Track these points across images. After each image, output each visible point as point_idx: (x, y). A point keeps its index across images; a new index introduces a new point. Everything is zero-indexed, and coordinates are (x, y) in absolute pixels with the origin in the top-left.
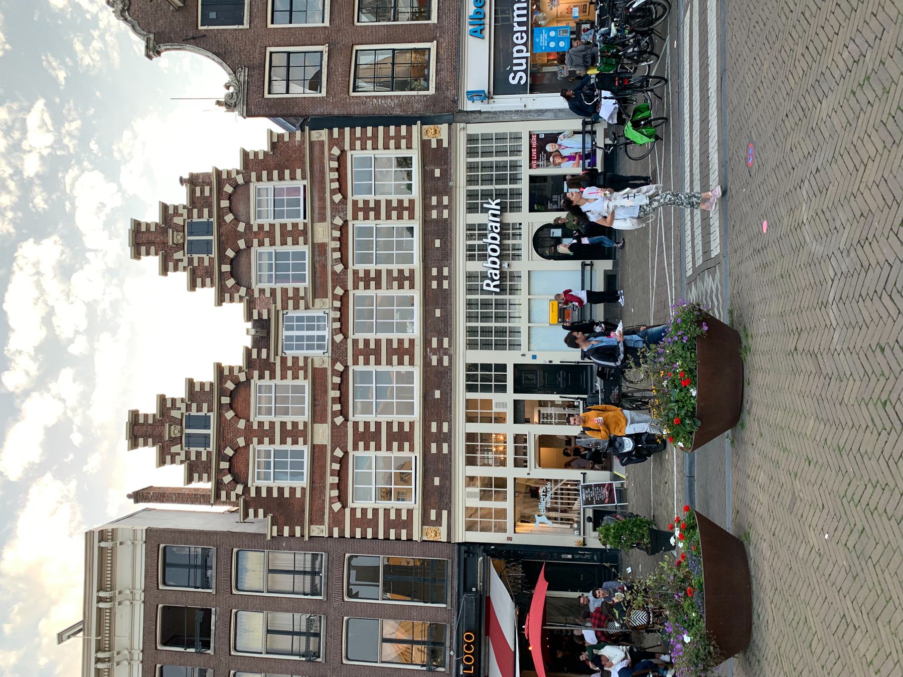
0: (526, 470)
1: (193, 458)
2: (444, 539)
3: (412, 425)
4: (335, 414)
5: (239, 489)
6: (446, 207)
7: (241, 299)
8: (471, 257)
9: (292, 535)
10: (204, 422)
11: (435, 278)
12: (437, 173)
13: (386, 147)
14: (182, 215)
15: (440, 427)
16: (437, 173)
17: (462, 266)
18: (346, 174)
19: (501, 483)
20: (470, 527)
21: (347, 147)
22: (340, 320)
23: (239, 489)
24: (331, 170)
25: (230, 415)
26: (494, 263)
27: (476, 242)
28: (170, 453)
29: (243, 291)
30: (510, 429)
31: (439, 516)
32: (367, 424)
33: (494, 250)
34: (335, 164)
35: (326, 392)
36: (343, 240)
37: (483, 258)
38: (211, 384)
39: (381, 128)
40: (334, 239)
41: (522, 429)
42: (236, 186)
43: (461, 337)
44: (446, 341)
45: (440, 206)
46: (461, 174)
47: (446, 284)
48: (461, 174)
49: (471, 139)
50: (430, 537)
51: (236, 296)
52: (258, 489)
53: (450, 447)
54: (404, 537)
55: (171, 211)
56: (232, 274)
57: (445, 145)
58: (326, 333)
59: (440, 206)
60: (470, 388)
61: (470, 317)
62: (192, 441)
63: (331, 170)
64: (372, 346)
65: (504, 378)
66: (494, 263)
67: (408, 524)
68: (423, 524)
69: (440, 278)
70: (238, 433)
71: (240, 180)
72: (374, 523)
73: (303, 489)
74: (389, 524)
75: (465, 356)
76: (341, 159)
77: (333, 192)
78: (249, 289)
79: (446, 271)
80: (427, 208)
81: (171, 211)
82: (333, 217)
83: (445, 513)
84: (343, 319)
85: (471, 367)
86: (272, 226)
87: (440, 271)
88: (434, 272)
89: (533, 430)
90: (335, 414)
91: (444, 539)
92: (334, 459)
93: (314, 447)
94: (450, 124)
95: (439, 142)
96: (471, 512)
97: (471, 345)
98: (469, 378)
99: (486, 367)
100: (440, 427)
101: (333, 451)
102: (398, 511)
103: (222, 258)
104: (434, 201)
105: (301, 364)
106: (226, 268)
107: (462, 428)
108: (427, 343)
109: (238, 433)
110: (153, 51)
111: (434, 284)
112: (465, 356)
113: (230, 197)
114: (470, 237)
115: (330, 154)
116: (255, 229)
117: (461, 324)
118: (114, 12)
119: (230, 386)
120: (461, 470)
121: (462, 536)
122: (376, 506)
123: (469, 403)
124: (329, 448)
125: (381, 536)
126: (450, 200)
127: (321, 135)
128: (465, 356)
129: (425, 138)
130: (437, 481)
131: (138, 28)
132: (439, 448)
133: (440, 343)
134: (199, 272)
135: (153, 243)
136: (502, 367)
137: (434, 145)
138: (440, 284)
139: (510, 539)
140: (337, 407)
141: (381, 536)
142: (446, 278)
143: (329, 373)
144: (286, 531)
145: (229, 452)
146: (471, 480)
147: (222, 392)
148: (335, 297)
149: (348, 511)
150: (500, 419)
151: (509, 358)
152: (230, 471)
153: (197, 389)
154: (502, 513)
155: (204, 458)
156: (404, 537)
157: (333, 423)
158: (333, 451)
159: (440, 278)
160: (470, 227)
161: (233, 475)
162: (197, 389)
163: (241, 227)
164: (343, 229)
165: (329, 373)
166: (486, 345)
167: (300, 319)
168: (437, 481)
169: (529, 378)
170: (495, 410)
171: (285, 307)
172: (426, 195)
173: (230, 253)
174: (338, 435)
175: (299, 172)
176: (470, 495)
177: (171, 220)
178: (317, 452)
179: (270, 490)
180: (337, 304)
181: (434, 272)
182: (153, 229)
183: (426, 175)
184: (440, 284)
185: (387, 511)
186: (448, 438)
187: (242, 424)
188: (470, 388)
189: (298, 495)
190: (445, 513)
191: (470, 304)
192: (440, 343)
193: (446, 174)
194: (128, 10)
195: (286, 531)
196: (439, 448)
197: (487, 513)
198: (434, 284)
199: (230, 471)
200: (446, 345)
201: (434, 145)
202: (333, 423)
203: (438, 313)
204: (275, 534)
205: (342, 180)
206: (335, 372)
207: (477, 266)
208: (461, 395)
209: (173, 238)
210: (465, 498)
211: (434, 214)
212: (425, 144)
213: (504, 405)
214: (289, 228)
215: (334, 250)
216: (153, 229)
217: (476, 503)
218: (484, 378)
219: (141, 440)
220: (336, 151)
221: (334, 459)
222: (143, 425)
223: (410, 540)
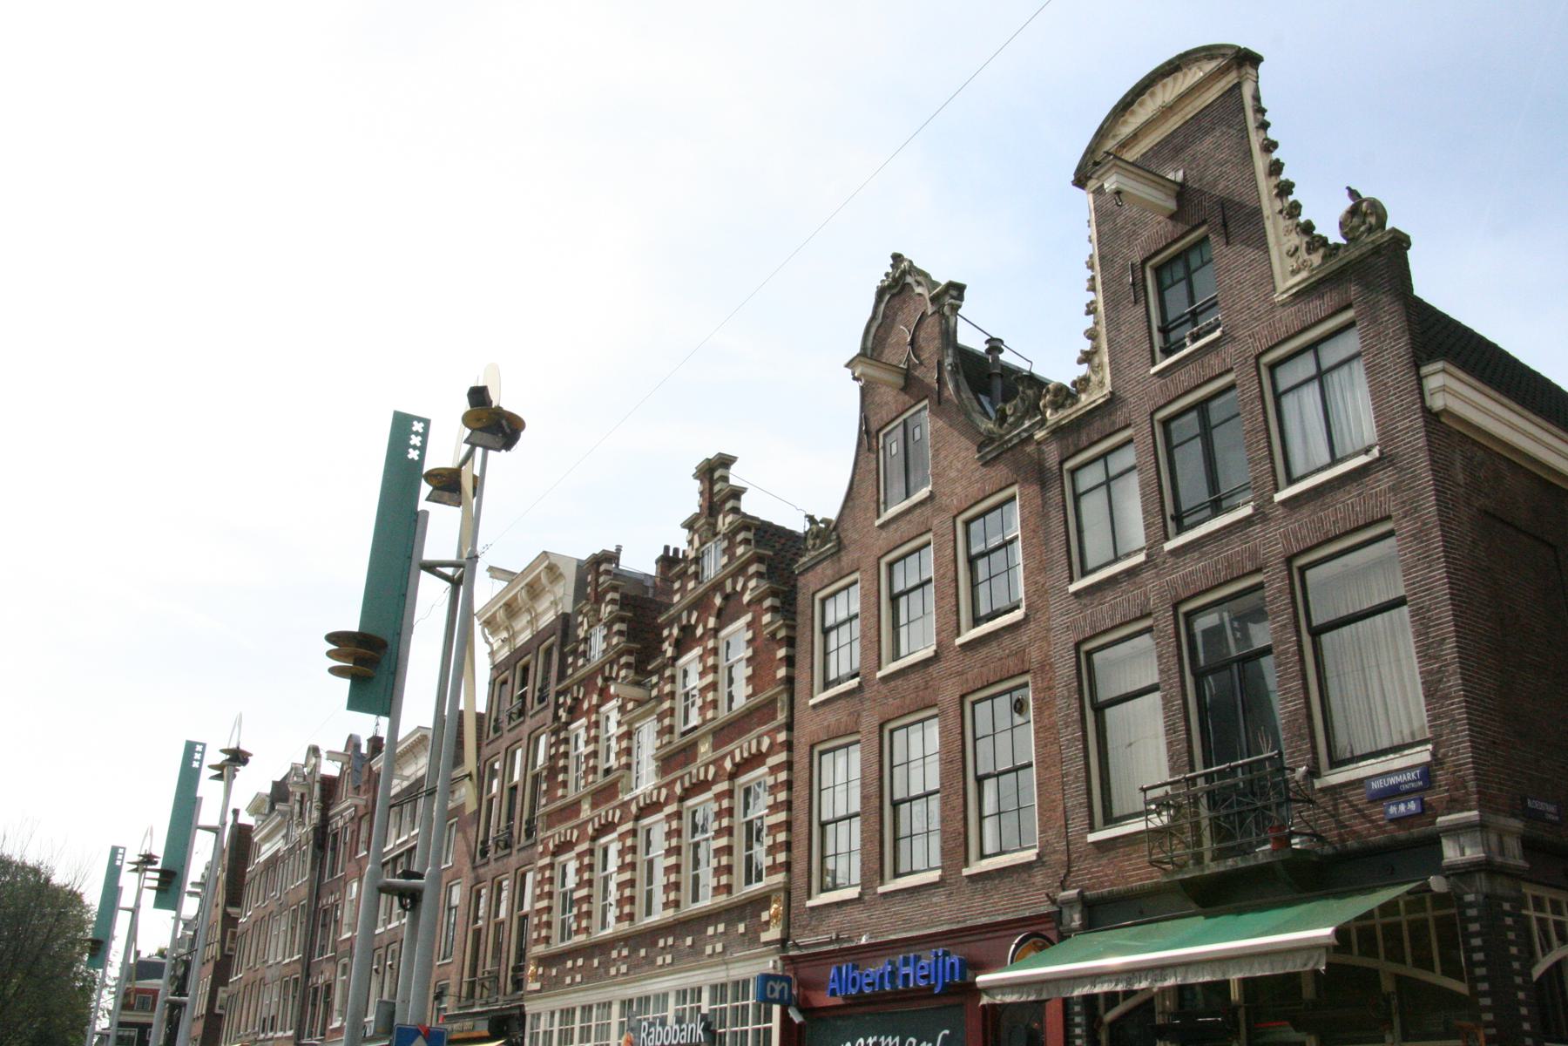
118: (887, 275)
131: (873, 330)
194: (893, 296)
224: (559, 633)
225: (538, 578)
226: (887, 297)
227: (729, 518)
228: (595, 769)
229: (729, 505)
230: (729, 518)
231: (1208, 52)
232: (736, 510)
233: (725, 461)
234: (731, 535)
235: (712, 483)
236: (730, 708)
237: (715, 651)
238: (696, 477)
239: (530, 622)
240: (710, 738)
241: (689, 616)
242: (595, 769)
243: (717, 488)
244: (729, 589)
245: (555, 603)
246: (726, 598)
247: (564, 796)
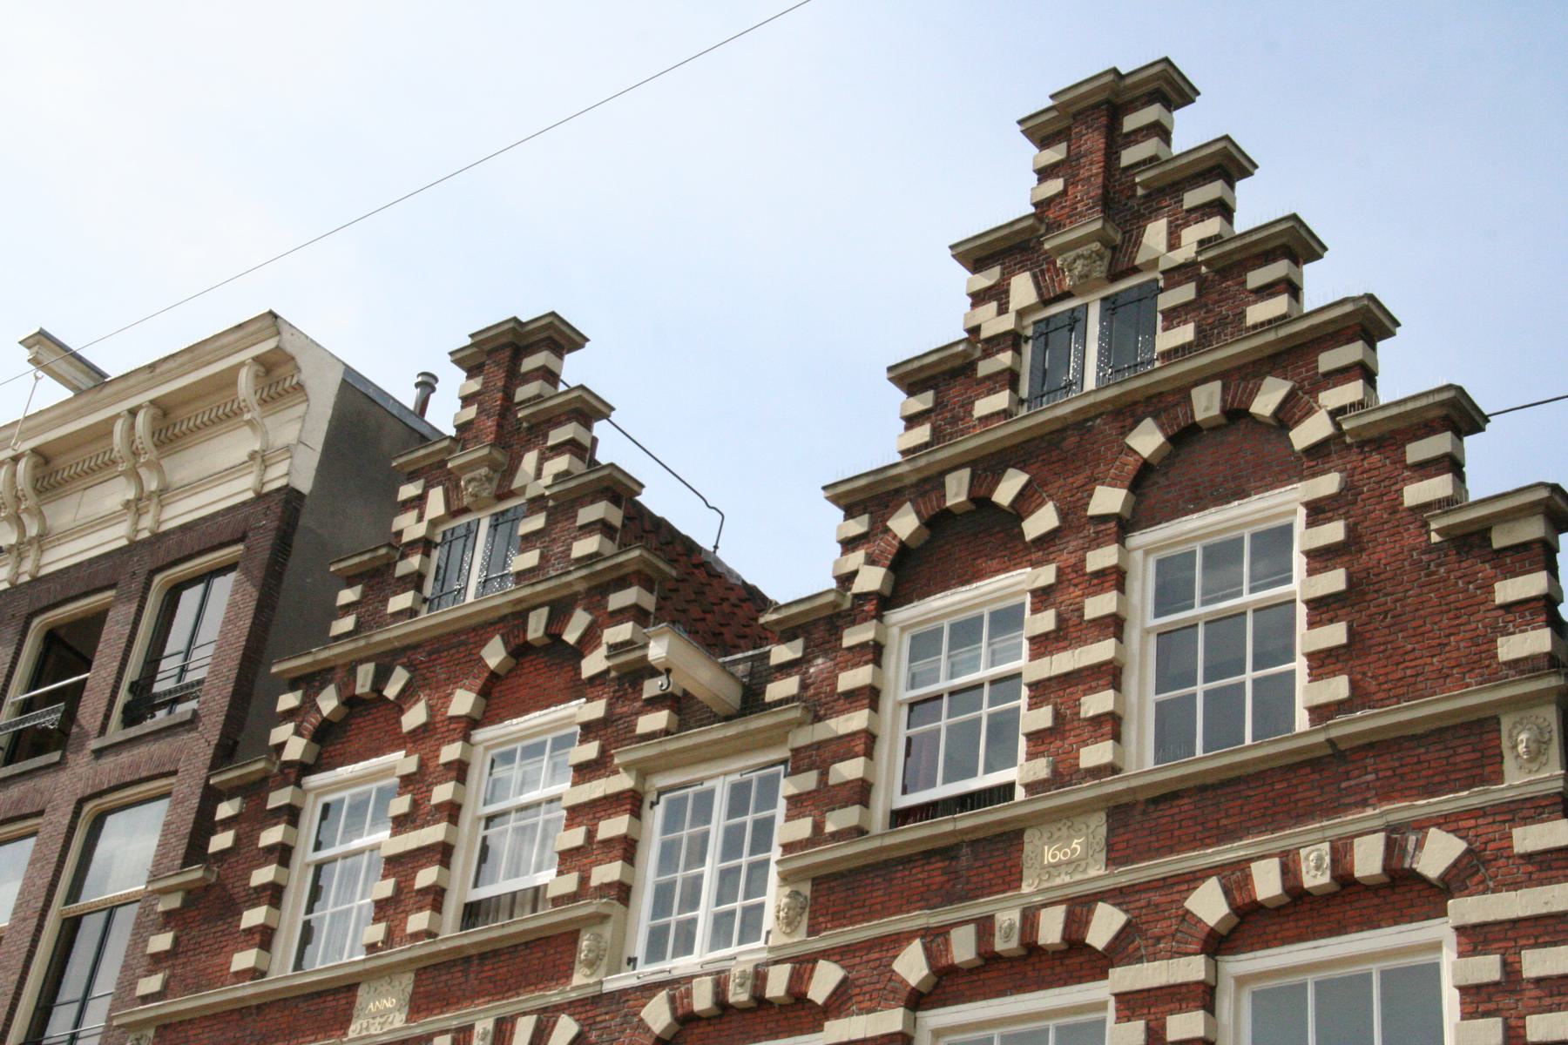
14: (1174, 243)
18: (1339, 929)
21: (1469, 908)
24: (1341, 852)
34: (1368, 860)
36: (1031, 966)
40: (1030, 918)
63: (1341, 852)
76: (1403, 893)
77: (1235, 878)
78: (884, 602)
113: (1235, 414)
115: (1421, 826)
143: (554, 996)
148: (803, 966)
164: (1076, 960)
165: (554, 996)
171: (799, 762)
180: (777, 984)
205: (1301, 913)
215: (985, 926)
220: (1437, 854)
224: (264, 544)
225: (227, 380)
227: (561, 463)
228: (435, 897)
229: (557, 436)
230: (561, 463)
232: (582, 450)
233: (558, 336)
234: (560, 506)
235: (514, 377)
236: (298, 965)
237: (459, 771)
238: (1040, 130)
239: (135, 507)
240: (407, 981)
241: (381, 677)
242: (435, 897)
243: (523, 392)
244: (363, 685)
245: (261, 458)
246: (351, 703)
247: (256, 973)
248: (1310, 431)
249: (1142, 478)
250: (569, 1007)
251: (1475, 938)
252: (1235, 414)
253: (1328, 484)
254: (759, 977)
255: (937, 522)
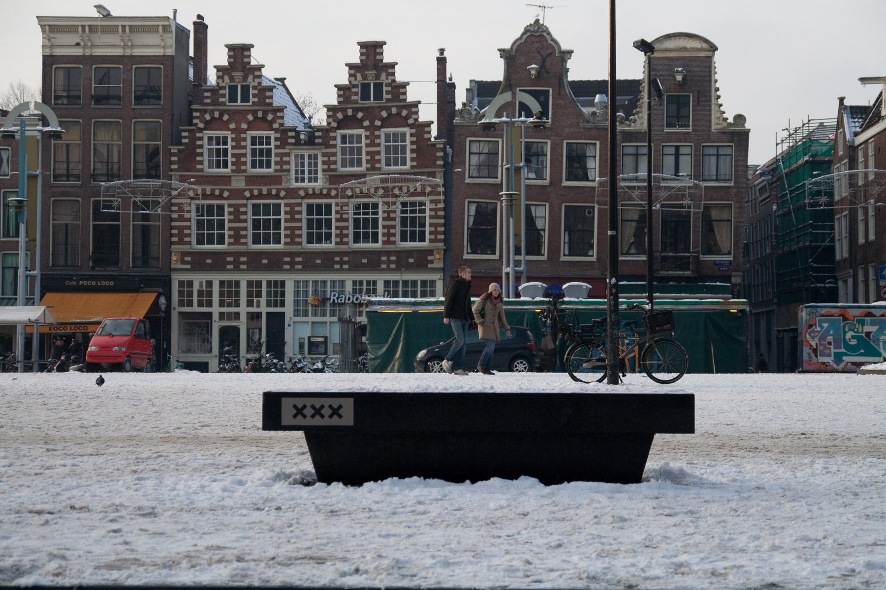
0: (217, 319)
1: (221, 92)
2: (173, 266)
3: (246, 244)
4: (251, 191)
5: (201, 125)
6: (388, 266)
7: (329, 124)
8: (355, 283)
9: (172, 163)
10: (245, 98)
11: (341, 259)
12: (411, 260)
13: (431, 225)
15: (243, 263)
16: (411, 260)
17: (349, 279)
19: (209, 304)
20: (181, 283)
22: (314, 193)
23: (201, 125)
25: (250, 117)
26: (349, 299)
27: (365, 287)
28: (224, 74)
29: (334, 125)
30: (243, 310)
31: (187, 263)
32: (245, 213)
33: (357, 299)
35: (265, 184)
37: (355, 291)
38: (271, 104)
39: (443, 221)
41: (243, 317)
42: (408, 117)
43: (302, 277)
44: (300, 267)
45: (389, 262)
46: (410, 277)
47: (337, 266)
48: (410, 277)
49: (433, 283)
50: (174, 258)
51: (331, 120)
52: (201, 139)
53: (231, 270)
54: (173, 239)
55: (390, 71)
56: (346, 117)
57: (430, 266)
58: (306, 184)
59: (389, 262)
60: (269, 283)
61: (315, 282)
62: (233, 90)
64: (297, 216)
65: (276, 306)
66: (349, 299)
67: (181, 242)
68: (182, 252)
69: (341, 263)
70: (238, 124)
71: (411, 121)
72: (181, 219)
73: (202, 170)
74: (181, 229)
75: (290, 280)
79: (346, 266)
80: (388, 253)
81: (390, 71)
82: (383, 188)
83: (189, 267)
84: (314, 195)
85: (283, 283)
86: (379, 145)
87: (346, 263)
88: (346, 259)
89: (242, 325)
90: (251, 191)
91: (173, 266)
92: (222, 191)
93: (230, 177)
94: (443, 269)
95: (432, 262)
96: (190, 284)
97: (297, 283)
98: (276, 282)
99: (283, 294)
100: (243, 263)
101: (228, 190)
102: (189, 235)
103: (356, 110)
104: (393, 258)
105: (285, 167)
106: (350, 112)
107: (243, 279)
108: (299, 254)
109: (238, 124)
110: (503, 53)
111: (337, 259)
112: (290, 280)
113: (399, 114)
114: (368, 283)
116: (377, 133)
117: (311, 277)
119: (270, 117)
120: (216, 278)
121: (176, 278)
122: (193, 220)
123: (259, 284)
124: (229, 187)
125: (173, 224)
126: (393, 269)
127: (439, 180)
128: (290, 279)
129: (435, 252)
130: (209, 261)
131: (518, 43)
132: (230, 263)
133: (298, 263)
134: (347, 93)
135: (367, 58)
136: (283, 304)
137: (430, 258)
138: (337, 263)
139: (175, 309)
140: (256, 193)
141: (173, 224)
142: (341, 267)
144: (174, 159)
145: (226, 117)
146: (209, 284)
147: (265, 113)
148: (329, 190)
149: (188, 201)
150: (250, 304)
151: (288, 309)
152: (213, 118)
153: (268, 94)
154: (190, 304)
155: (222, 100)
156: (173, 239)
157: (245, 190)
158: (228, 190)
159: (341, 263)
160: (375, 283)
161: (210, 121)
162: (268, 94)
163: (378, 123)
166: (297, 293)
167: (316, 165)
168: (209, 261)
169: (276, 322)
170: (255, 300)
172: (398, 253)
173: (360, 115)
174: (237, 194)
175: (415, 163)
176: (201, 283)
177: (384, 71)
178: (226, 179)
179: (201, 146)
181: (346, 259)
182: (378, 57)
183: (410, 253)
184: (337, 263)
185: (189, 228)
186: (237, 269)
187: (244, 126)
188: (269, 283)
189: (198, 167)
190: (189, 267)
191: (324, 282)
192: (298, 263)
193: (410, 268)
195: (174, 159)
196: (230, 263)
197: (190, 294)
198: (337, 259)
199: (213, 118)
200: (297, 267)
201: (430, 258)
202: (245, 190)
203: (318, 261)
204: (172, 151)
206: (279, 191)
207: (349, 287)
208: (264, 277)
209: (371, 73)
210: (198, 279)
211: (384, 258)
212: (430, 252)
213: (258, 306)
214: (377, 157)
216: (378, 57)
217: (196, 288)
218: (277, 292)
219: (232, 53)
221: (222, 191)
222: (242, 54)
223: (172, 243)
226: (529, 34)
231: (706, 41)
248: (411, 121)
249: (383, 120)
250: (283, 189)
251: (432, 202)
252: (399, 114)
253: (414, 131)
254: (321, 190)
255: (346, 117)
